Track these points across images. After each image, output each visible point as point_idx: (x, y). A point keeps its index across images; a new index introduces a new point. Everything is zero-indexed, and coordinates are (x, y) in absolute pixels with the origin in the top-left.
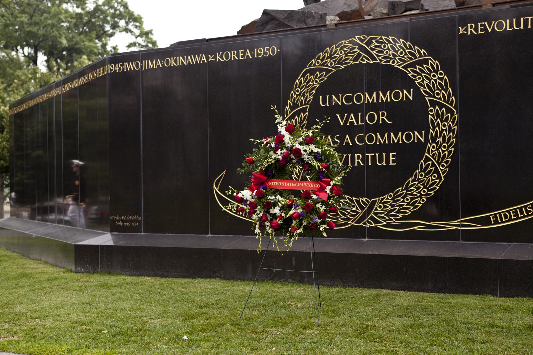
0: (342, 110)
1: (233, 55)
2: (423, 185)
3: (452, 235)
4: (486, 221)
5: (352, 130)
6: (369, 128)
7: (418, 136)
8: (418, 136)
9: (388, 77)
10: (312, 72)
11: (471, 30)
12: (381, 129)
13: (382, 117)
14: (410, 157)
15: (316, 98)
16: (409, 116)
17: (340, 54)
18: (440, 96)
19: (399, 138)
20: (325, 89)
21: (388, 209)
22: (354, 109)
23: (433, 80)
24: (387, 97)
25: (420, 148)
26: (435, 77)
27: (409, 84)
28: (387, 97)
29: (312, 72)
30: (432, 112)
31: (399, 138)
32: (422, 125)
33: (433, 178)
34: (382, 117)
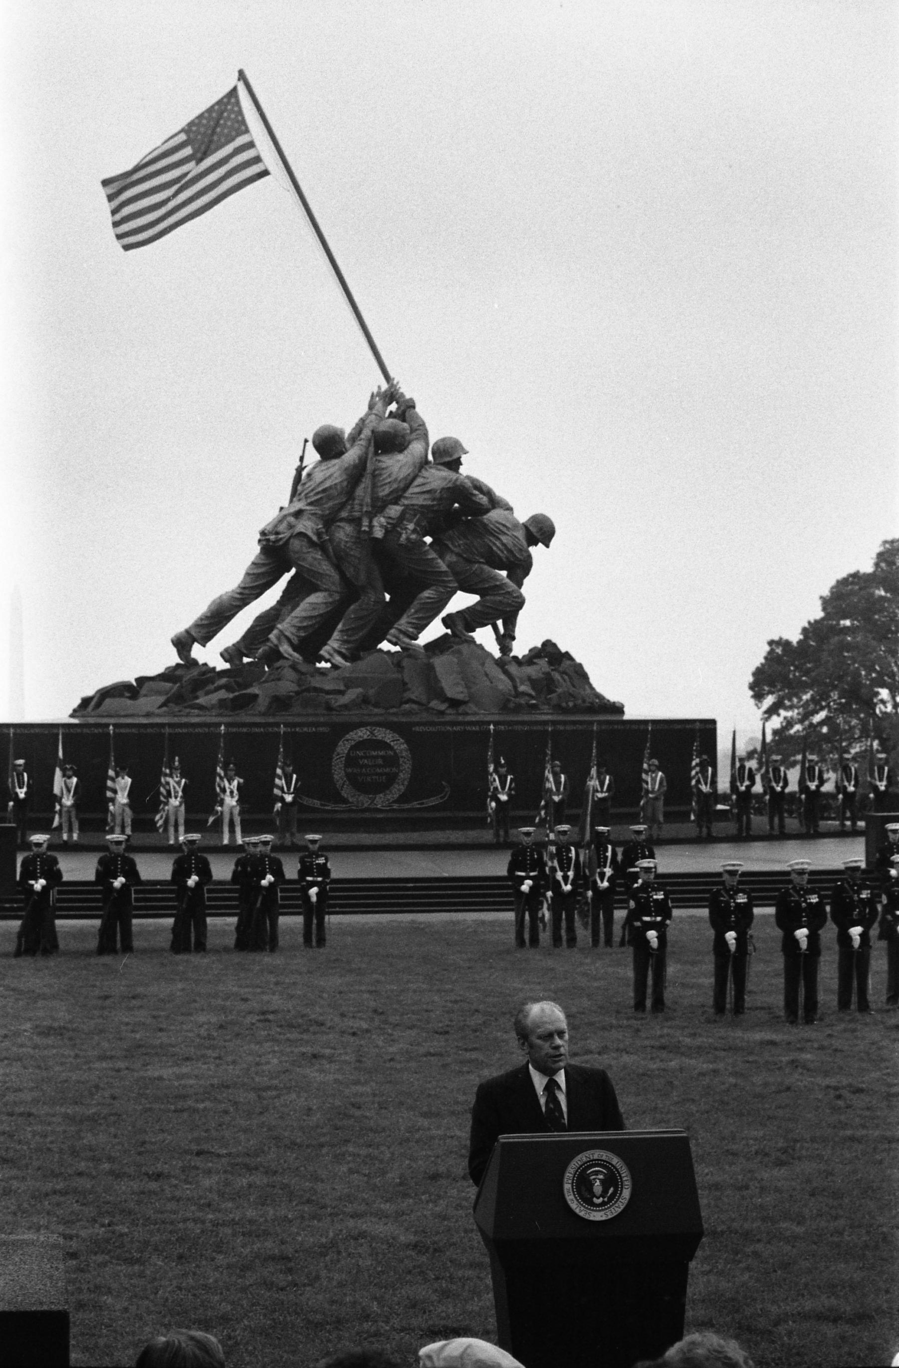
0: (362, 758)
1: (305, 729)
2: (397, 789)
3: (409, 810)
4: (423, 804)
5: (366, 766)
7: (394, 769)
8: (394, 769)
10: (347, 740)
11: (417, 729)
12: (380, 766)
13: (380, 761)
14: (392, 779)
15: (349, 751)
17: (360, 734)
19: (387, 770)
20: (353, 748)
21: (380, 801)
22: (366, 757)
23: (401, 746)
24: (382, 753)
25: (396, 775)
26: (402, 747)
27: (391, 748)
28: (382, 753)
29: (347, 740)
30: (401, 760)
31: (387, 770)
33: (402, 787)
34: (380, 761)
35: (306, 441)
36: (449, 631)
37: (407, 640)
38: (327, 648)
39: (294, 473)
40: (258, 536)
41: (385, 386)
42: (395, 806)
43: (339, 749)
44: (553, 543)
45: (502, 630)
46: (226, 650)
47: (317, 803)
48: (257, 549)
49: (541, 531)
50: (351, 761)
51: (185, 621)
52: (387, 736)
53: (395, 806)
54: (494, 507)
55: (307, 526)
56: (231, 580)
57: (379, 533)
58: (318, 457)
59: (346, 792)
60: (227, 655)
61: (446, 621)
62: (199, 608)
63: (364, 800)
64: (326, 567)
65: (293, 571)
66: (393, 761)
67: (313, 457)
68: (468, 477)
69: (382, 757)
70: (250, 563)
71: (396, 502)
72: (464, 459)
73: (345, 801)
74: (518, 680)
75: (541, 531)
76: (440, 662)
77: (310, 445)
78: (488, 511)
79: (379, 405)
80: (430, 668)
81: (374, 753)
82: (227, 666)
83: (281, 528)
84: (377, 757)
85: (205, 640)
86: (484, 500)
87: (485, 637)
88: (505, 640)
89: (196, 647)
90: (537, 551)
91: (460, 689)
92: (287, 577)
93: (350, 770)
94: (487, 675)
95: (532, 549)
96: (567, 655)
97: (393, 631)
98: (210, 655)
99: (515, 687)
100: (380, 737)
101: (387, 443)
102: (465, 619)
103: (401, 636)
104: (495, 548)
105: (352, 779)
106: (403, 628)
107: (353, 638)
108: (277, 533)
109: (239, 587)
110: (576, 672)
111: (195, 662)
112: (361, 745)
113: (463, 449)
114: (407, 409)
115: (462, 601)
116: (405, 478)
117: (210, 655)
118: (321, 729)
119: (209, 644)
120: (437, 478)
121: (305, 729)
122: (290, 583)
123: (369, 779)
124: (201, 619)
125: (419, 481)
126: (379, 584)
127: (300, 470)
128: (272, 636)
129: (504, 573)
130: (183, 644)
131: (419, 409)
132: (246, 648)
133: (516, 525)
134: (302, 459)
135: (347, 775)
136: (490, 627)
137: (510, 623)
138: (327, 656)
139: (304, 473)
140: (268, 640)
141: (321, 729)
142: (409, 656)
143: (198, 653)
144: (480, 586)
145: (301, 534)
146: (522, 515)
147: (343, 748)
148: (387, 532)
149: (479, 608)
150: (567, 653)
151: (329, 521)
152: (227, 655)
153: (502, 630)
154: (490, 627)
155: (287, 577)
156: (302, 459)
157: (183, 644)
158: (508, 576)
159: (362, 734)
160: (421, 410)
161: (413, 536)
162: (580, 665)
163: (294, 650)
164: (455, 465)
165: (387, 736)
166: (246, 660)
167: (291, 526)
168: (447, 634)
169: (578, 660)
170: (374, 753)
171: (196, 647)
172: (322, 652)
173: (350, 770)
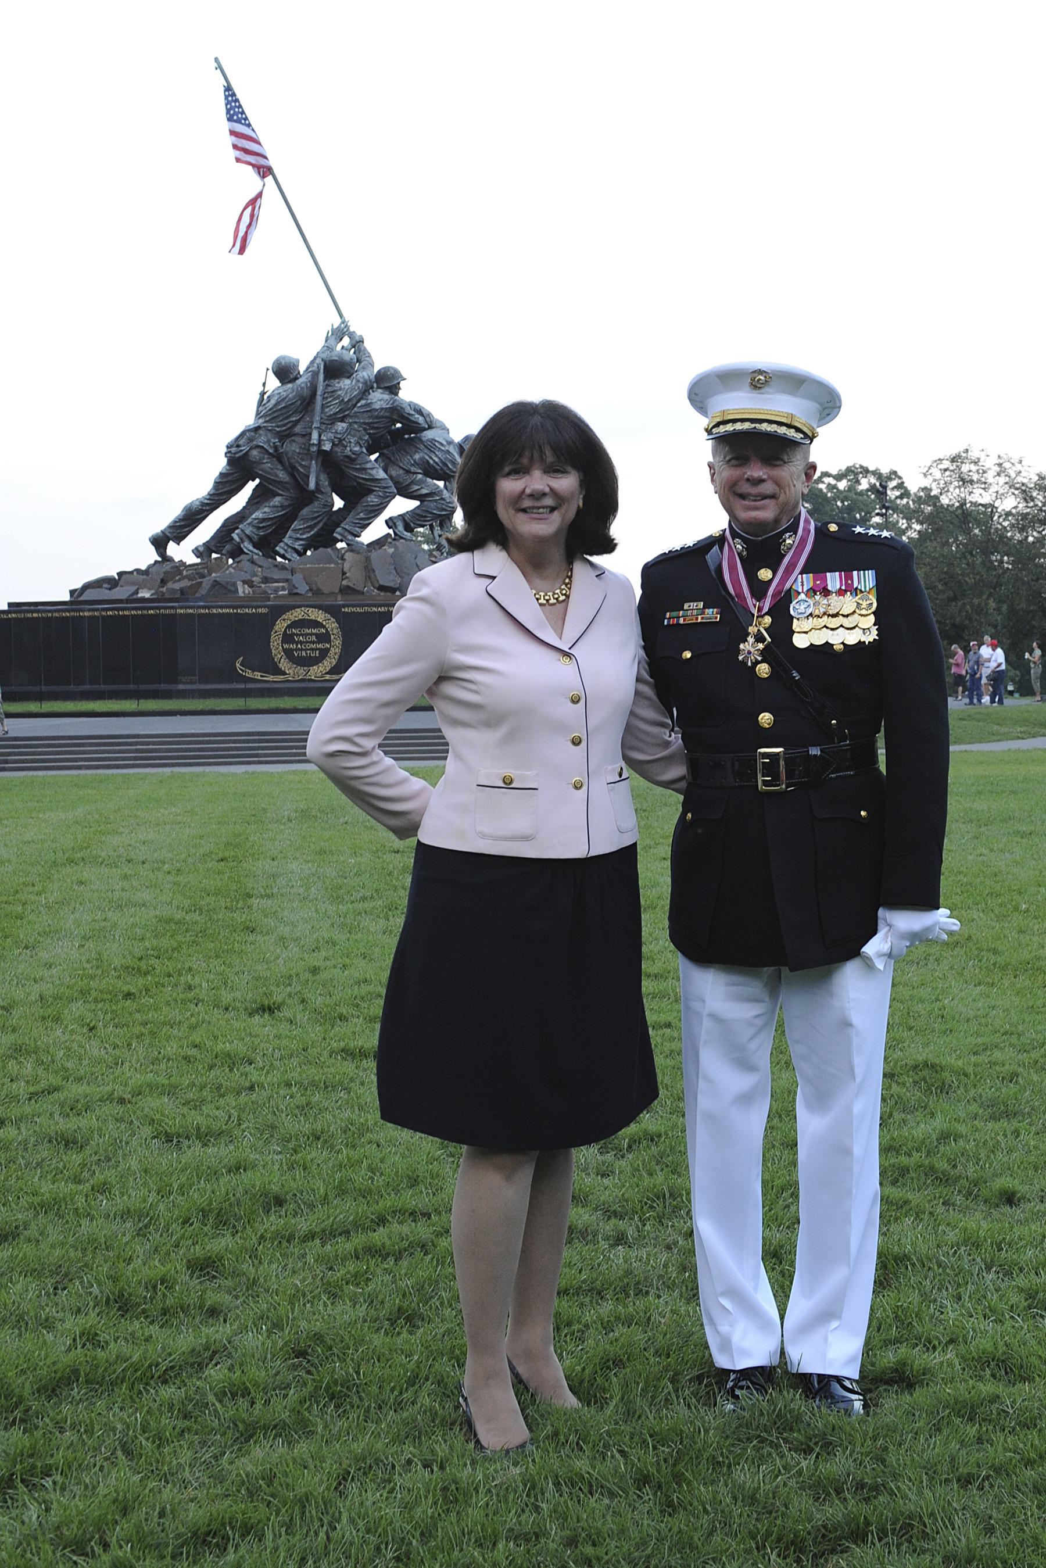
0: (297, 635)
5: (301, 643)
6: (307, 642)
9: (316, 624)
12: (313, 642)
14: (324, 653)
16: (325, 638)
18: (335, 632)
19: (320, 646)
20: (289, 627)
22: (302, 635)
23: (332, 625)
25: (328, 650)
27: (324, 627)
31: (320, 646)
32: (329, 641)
34: (314, 638)
36: (391, 531)
37: (350, 537)
38: (282, 544)
39: (258, 396)
40: (225, 450)
41: (337, 322)
42: (328, 677)
43: (276, 628)
46: (196, 548)
47: (258, 675)
50: (287, 638)
52: (320, 616)
53: (328, 677)
54: (430, 427)
55: (262, 440)
56: (202, 488)
57: (327, 447)
58: (278, 383)
59: (284, 664)
60: (197, 552)
61: (390, 523)
62: (173, 512)
63: (300, 672)
64: (282, 475)
65: (257, 481)
66: (325, 638)
67: (274, 383)
68: (410, 404)
69: (316, 635)
70: (218, 474)
71: (342, 420)
72: (402, 384)
73: (284, 673)
76: (374, 555)
77: (270, 372)
78: (425, 429)
79: (332, 341)
80: (368, 559)
81: (308, 631)
82: (199, 560)
83: (241, 442)
84: (312, 634)
85: (179, 539)
86: (421, 420)
89: (171, 545)
91: (392, 577)
92: (251, 485)
93: (286, 646)
97: (339, 530)
98: (183, 552)
100: (313, 617)
101: (334, 369)
102: (404, 520)
103: (346, 534)
104: (431, 462)
105: (288, 653)
106: (347, 527)
107: (304, 536)
108: (238, 446)
109: (209, 494)
111: (170, 560)
112: (295, 624)
113: (401, 376)
114: (357, 343)
115: (401, 506)
116: (349, 400)
118: (260, 610)
119: (182, 543)
120: (378, 398)
121: (247, 610)
122: (254, 490)
123: (304, 654)
124: (175, 522)
125: (363, 402)
126: (329, 489)
127: (263, 394)
128: (235, 536)
129: (441, 484)
131: (365, 344)
132: (216, 547)
133: (450, 443)
134: (264, 384)
135: (284, 650)
138: (282, 552)
139: (265, 397)
140: (233, 539)
141: (260, 610)
142: (352, 551)
143: (173, 550)
144: (419, 493)
145: (258, 446)
147: (281, 625)
148: (334, 444)
149: (418, 511)
151: (285, 436)
152: (197, 552)
155: (251, 485)
156: (264, 384)
157: (159, 543)
158: (445, 486)
159: (298, 614)
160: (368, 345)
161: (357, 449)
163: (254, 547)
164: (394, 389)
165: (320, 616)
166: (214, 555)
167: (250, 440)
168: (388, 535)
170: (308, 631)
171: (171, 545)
172: (277, 548)
173: (286, 646)
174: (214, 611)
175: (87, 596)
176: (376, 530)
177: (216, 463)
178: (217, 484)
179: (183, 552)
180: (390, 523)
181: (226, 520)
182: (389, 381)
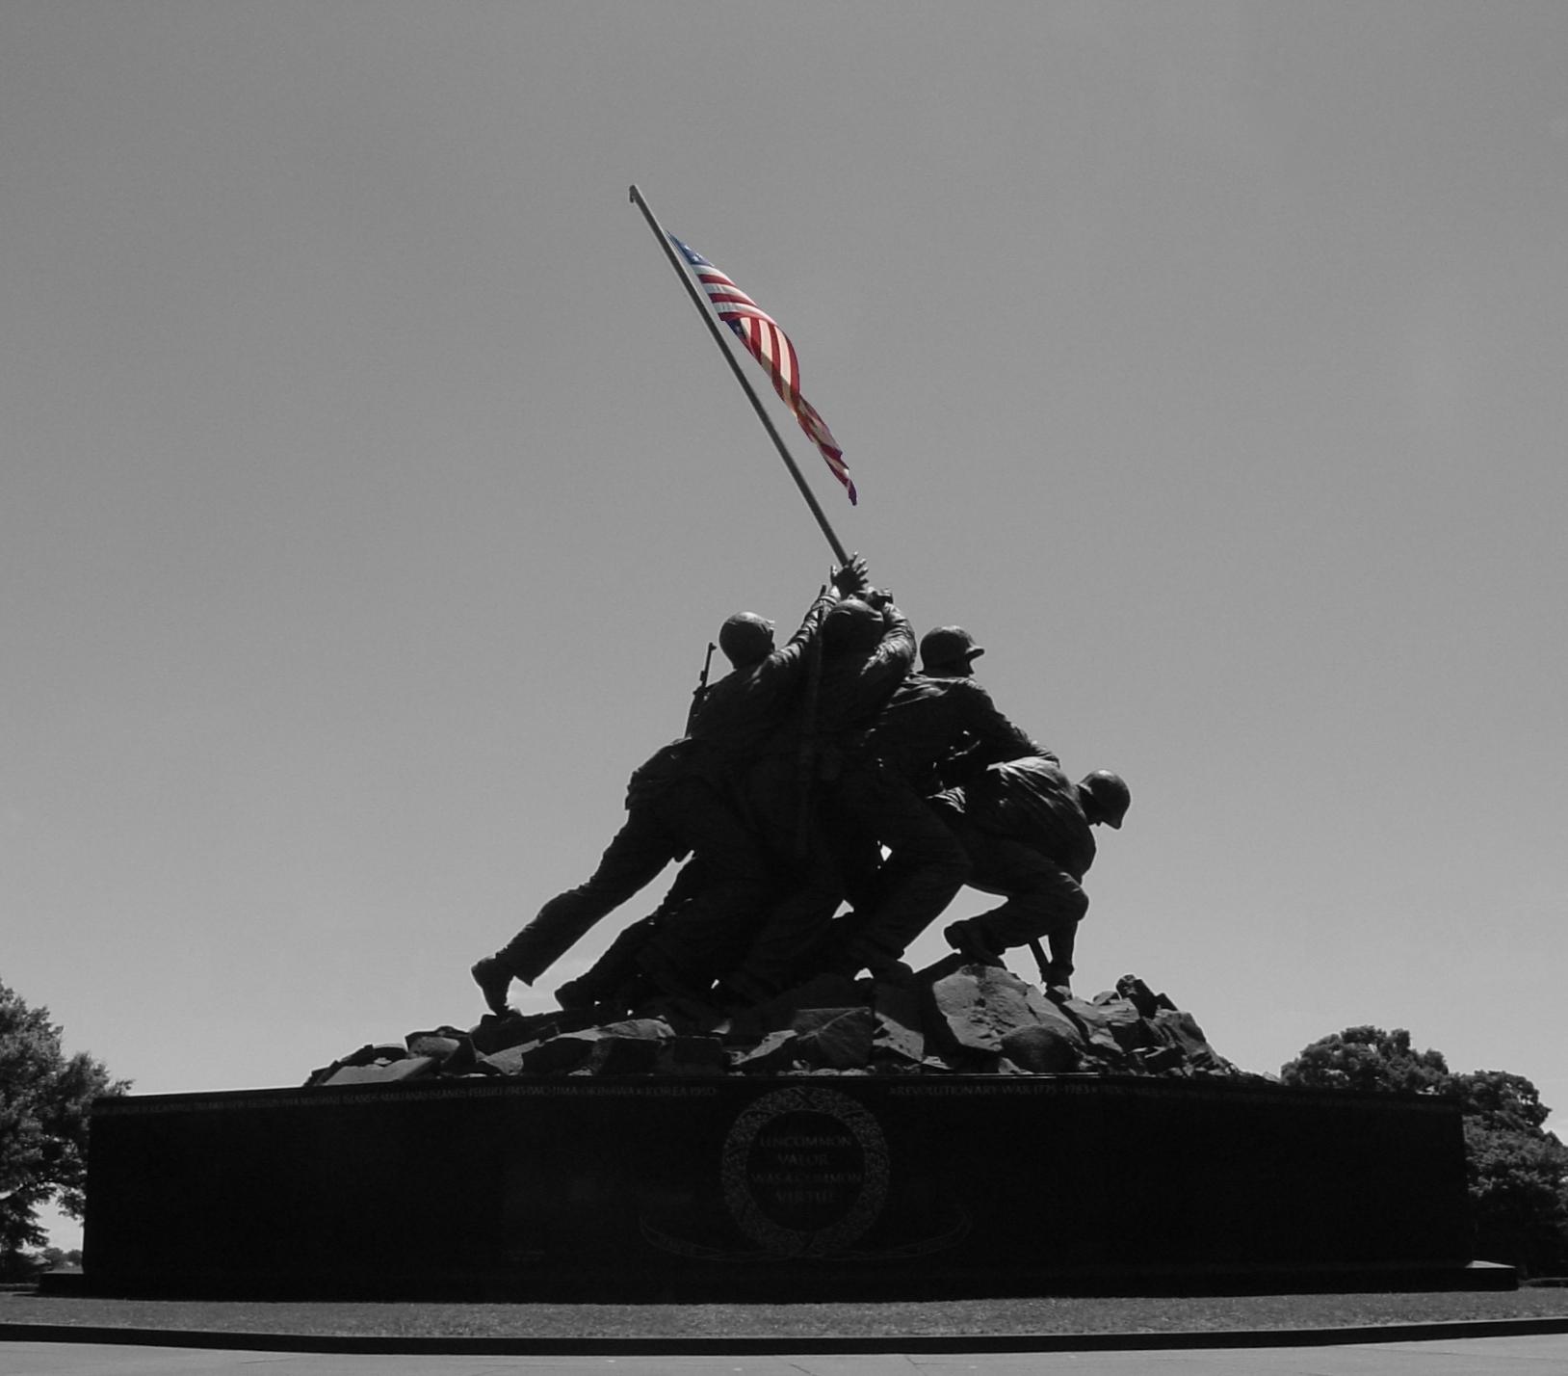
10: (754, 1114)
29: (754, 1114)
35: (712, 647)
44: (1127, 817)
45: (1050, 958)
48: (623, 817)
49: (1108, 800)
51: (495, 942)
56: (580, 869)
60: (562, 994)
61: (954, 934)
67: (722, 668)
74: (1089, 1026)
75: (1108, 800)
77: (719, 652)
87: (1020, 962)
88: (1057, 971)
90: (1100, 832)
94: (1031, 1010)
95: (1093, 828)
96: (1164, 1002)
99: (1086, 1037)
101: (847, 633)
110: (1182, 1027)
111: (515, 1014)
117: (533, 998)
122: (681, 875)
127: (699, 693)
130: (493, 976)
133: (1063, 783)
134: (704, 676)
136: (1027, 947)
137: (1063, 946)
146: (1076, 776)
150: (1163, 996)
152: (564, 994)
153: (1050, 958)
154: (1027, 947)
156: (704, 676)
157: (493, 976)
162: (1189, 1017)
169: (1182, 1008)
174: (591, 1092)
175: (336, 1080)
176: (926, 949)
177: (610, 818)
178: (610, 856)
179: (533, 998)
180: (954, 934)
181: (625, 933)
182: (949, 652)
